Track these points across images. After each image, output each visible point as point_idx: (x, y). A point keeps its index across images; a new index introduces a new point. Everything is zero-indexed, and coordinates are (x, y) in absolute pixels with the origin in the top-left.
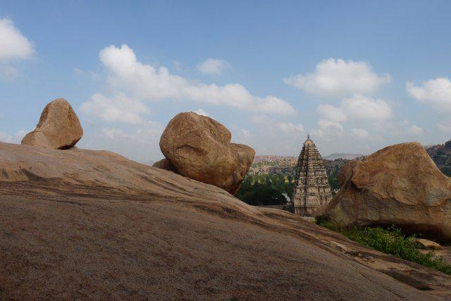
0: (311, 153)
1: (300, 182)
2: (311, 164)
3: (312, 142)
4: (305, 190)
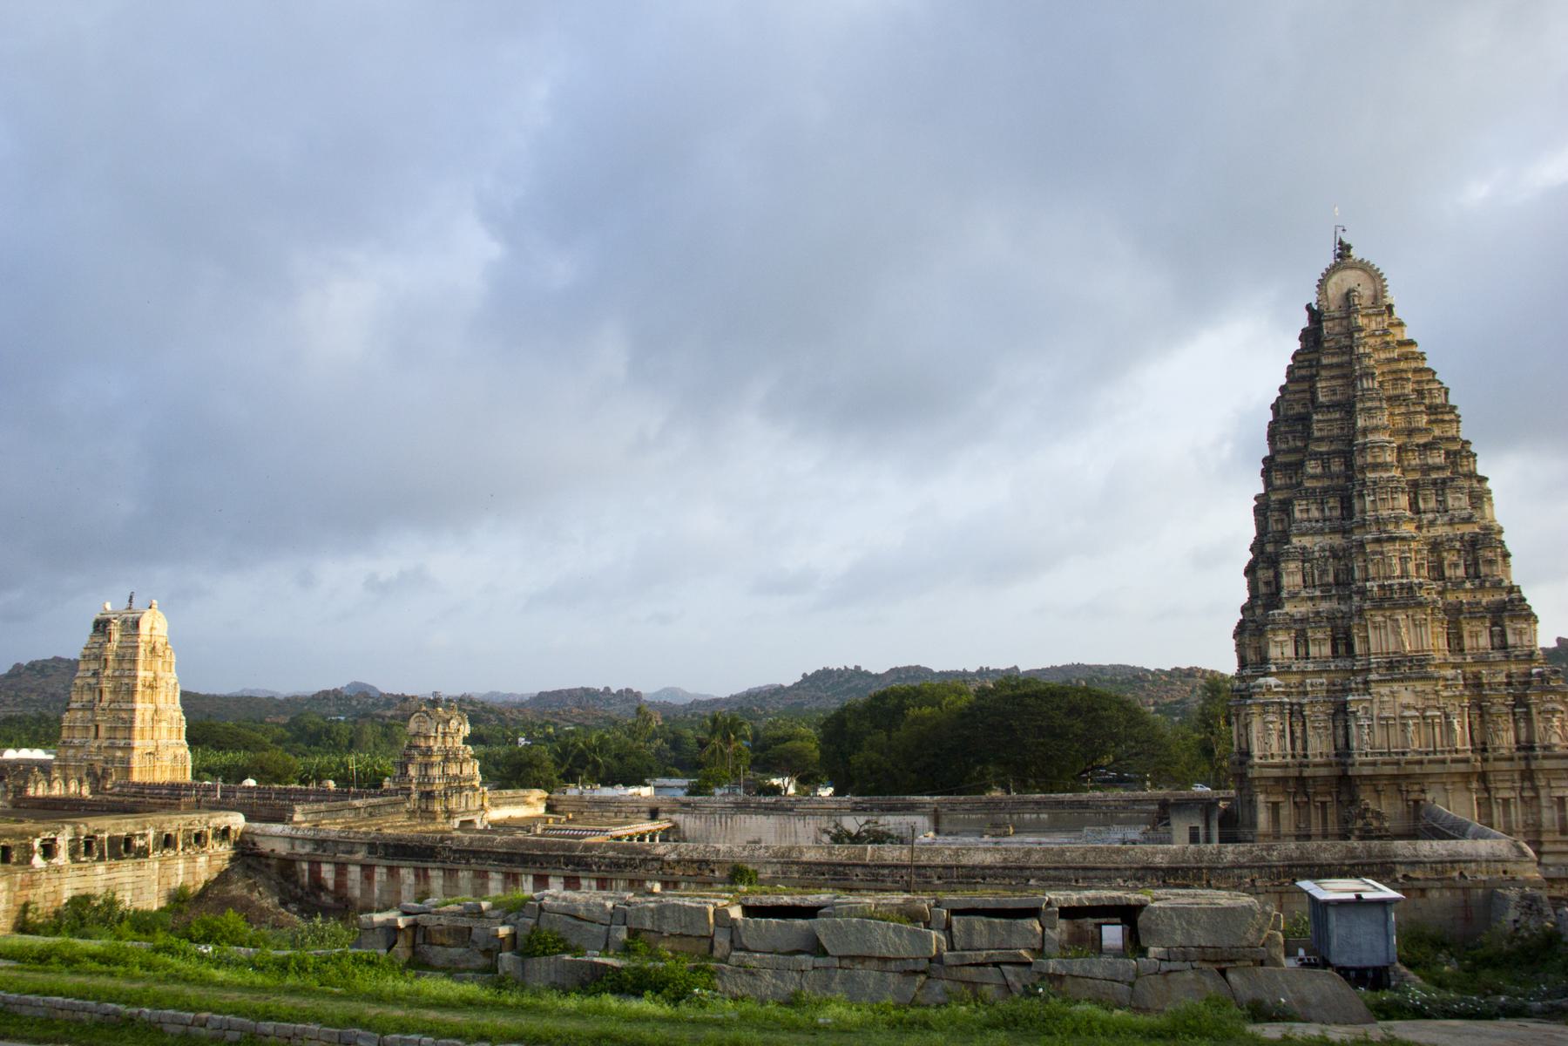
0: (1373, 356)
1: (1291, 578)
2: (1381, 428)
3: (1364, 267)
4: (1343, 642)
